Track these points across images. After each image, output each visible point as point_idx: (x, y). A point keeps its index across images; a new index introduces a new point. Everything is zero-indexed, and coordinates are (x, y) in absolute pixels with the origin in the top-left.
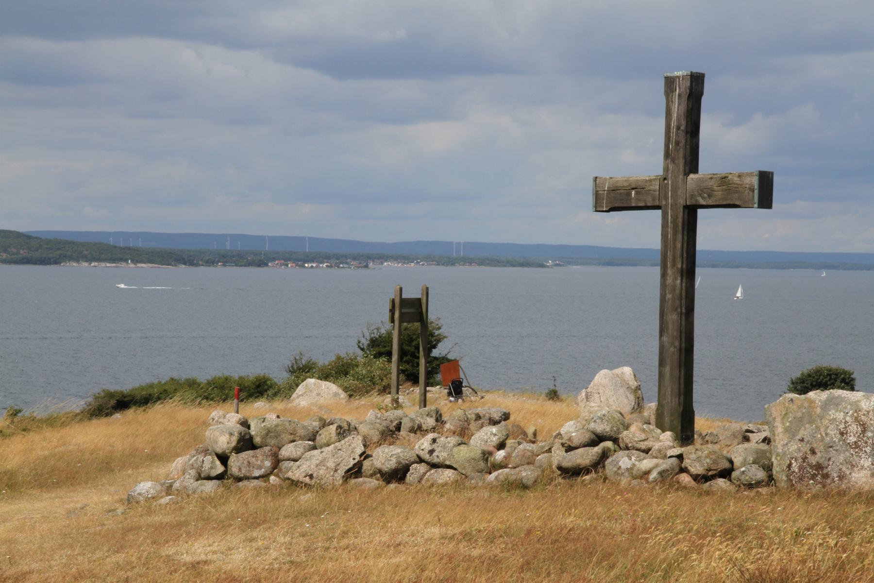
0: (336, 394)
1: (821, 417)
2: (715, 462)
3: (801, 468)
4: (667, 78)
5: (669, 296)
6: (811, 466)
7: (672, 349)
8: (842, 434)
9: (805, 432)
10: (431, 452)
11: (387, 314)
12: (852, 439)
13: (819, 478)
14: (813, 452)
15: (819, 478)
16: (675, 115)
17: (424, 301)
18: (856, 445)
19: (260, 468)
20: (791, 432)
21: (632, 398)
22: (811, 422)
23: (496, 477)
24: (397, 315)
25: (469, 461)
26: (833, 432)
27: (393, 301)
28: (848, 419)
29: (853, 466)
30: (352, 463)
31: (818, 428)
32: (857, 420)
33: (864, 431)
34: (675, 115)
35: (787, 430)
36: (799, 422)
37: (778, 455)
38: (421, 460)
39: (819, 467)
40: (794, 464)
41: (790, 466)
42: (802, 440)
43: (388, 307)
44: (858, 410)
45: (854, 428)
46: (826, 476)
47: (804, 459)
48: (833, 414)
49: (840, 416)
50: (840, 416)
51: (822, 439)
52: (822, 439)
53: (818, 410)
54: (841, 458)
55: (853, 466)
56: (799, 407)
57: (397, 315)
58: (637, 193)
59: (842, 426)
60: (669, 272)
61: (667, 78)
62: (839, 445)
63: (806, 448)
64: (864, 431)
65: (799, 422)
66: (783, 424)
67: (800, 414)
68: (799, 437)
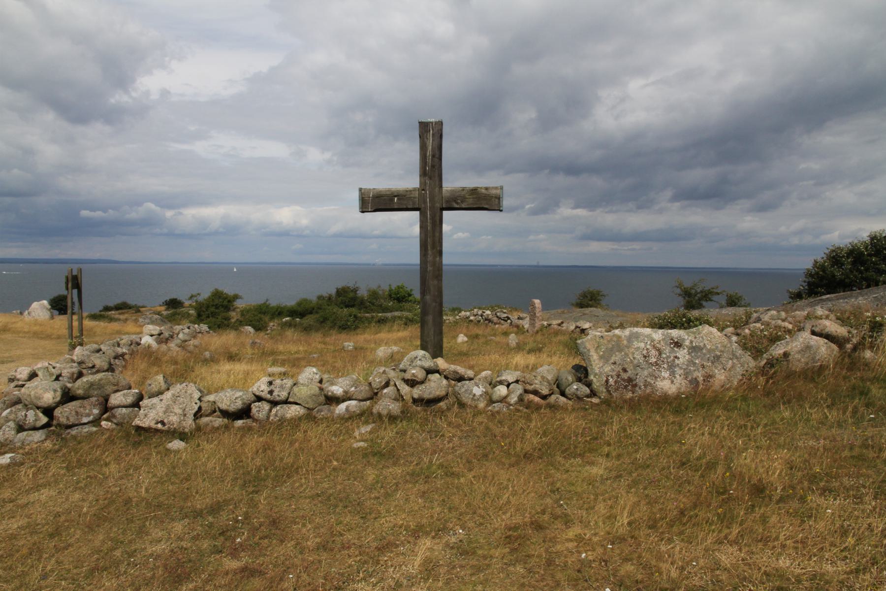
1: (628, 347)
3: (616, 382)
4: (421, 123)
5: (430, 268)
6: (624, 380)
7: (434, 304)
8: (645, 357)
9: (617, 357)
10: (271, 392)
11: (64, 286)
12: (653, 360)
13: (629, 387)
14: (625, 370)
15: (629, 387)
16: (430, 148)
17: (79, 276)
18: (656, 364)
19: (88, 415)
20: (605, 358)
22: (620, 351)
23: (347, 407)
24: (70, 285)
25: (311, 397)
26: (639, 357)
27: (67, 278)
28: (648, 347)
29: (656, 378)
31: (627, 355)
32: (654, 347)
33: (660, 354)
34: (430, 148)
35: (601, 357)
36: (611, 351)
37: (596, 375)
38: (259, 399)
39: (630, 380)
40: (611, 380)
41: (607, 381)
42: (615, 363)
43: (64, 280)
44: (653, 340)
45: (653, 352)
47: (618, 376)
48: (636, 344)
49: (642, 345)
50: (642, 345)
51: (632, 362)
52: (632, 362)
53: (625, 342)
54: (646, 373)
55: (656, 378)
56: (609, 341)
57: (70, 285)
58: (398, 199)
59: (645, 352)
60: (430, 252)
61: (421, 123)
62: (644, 365)
63: (619, 368)
64: (660, 354)
65: (611, 351)
66: (598, 353)
67: (610, 346)
68: (612, 361)
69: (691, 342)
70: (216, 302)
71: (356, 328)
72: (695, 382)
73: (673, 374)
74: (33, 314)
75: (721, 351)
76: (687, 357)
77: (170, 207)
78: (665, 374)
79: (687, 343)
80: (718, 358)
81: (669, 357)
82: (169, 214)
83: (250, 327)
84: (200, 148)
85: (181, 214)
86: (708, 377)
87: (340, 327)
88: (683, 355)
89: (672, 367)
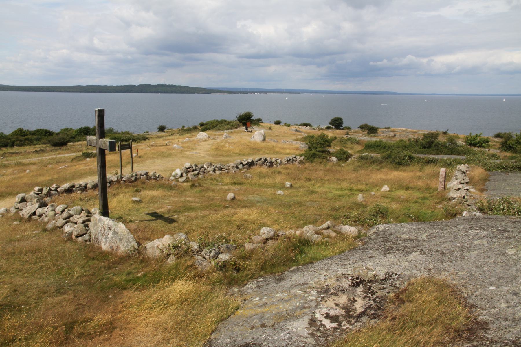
0: (206, 135)
2: (81, 232)
10: (46, 211)
12: (102, 233)
21: (263, 137)
30: (33, 211)
32: (103, 227)
33: (104, 231)
45: (103, 230)
46: (99, 242)
64: (104, 231)
69: (115, 229)
70: (318, 141)
71: (408, 165)
72: (112, 247)
73: (106, 241)
74: (255, 138)
75: (122, 237)
76: (112, 235)
77: (424, 56)
78: (104, 240)
79: (113, 229)
80: (121, 240)
81: (106, 233)
82: (425, 60)
83: (335, 158)
84: (446, 12)
85: (433, 60)
86: (118, 248)
87: (396, 163)
88: (111, 233)
89: (106, 238)
